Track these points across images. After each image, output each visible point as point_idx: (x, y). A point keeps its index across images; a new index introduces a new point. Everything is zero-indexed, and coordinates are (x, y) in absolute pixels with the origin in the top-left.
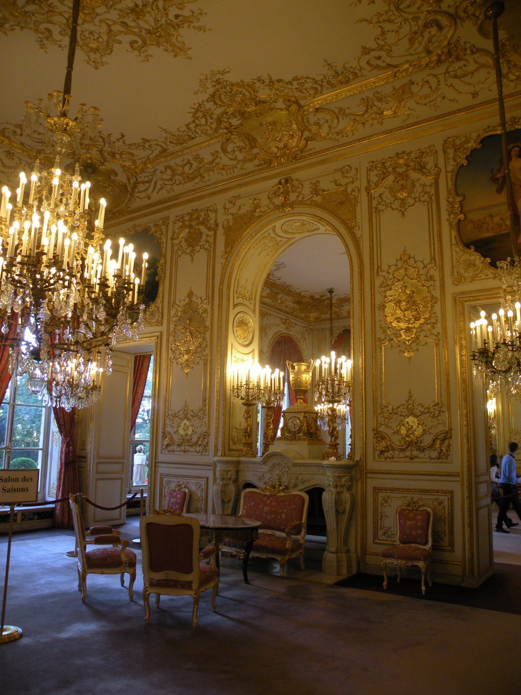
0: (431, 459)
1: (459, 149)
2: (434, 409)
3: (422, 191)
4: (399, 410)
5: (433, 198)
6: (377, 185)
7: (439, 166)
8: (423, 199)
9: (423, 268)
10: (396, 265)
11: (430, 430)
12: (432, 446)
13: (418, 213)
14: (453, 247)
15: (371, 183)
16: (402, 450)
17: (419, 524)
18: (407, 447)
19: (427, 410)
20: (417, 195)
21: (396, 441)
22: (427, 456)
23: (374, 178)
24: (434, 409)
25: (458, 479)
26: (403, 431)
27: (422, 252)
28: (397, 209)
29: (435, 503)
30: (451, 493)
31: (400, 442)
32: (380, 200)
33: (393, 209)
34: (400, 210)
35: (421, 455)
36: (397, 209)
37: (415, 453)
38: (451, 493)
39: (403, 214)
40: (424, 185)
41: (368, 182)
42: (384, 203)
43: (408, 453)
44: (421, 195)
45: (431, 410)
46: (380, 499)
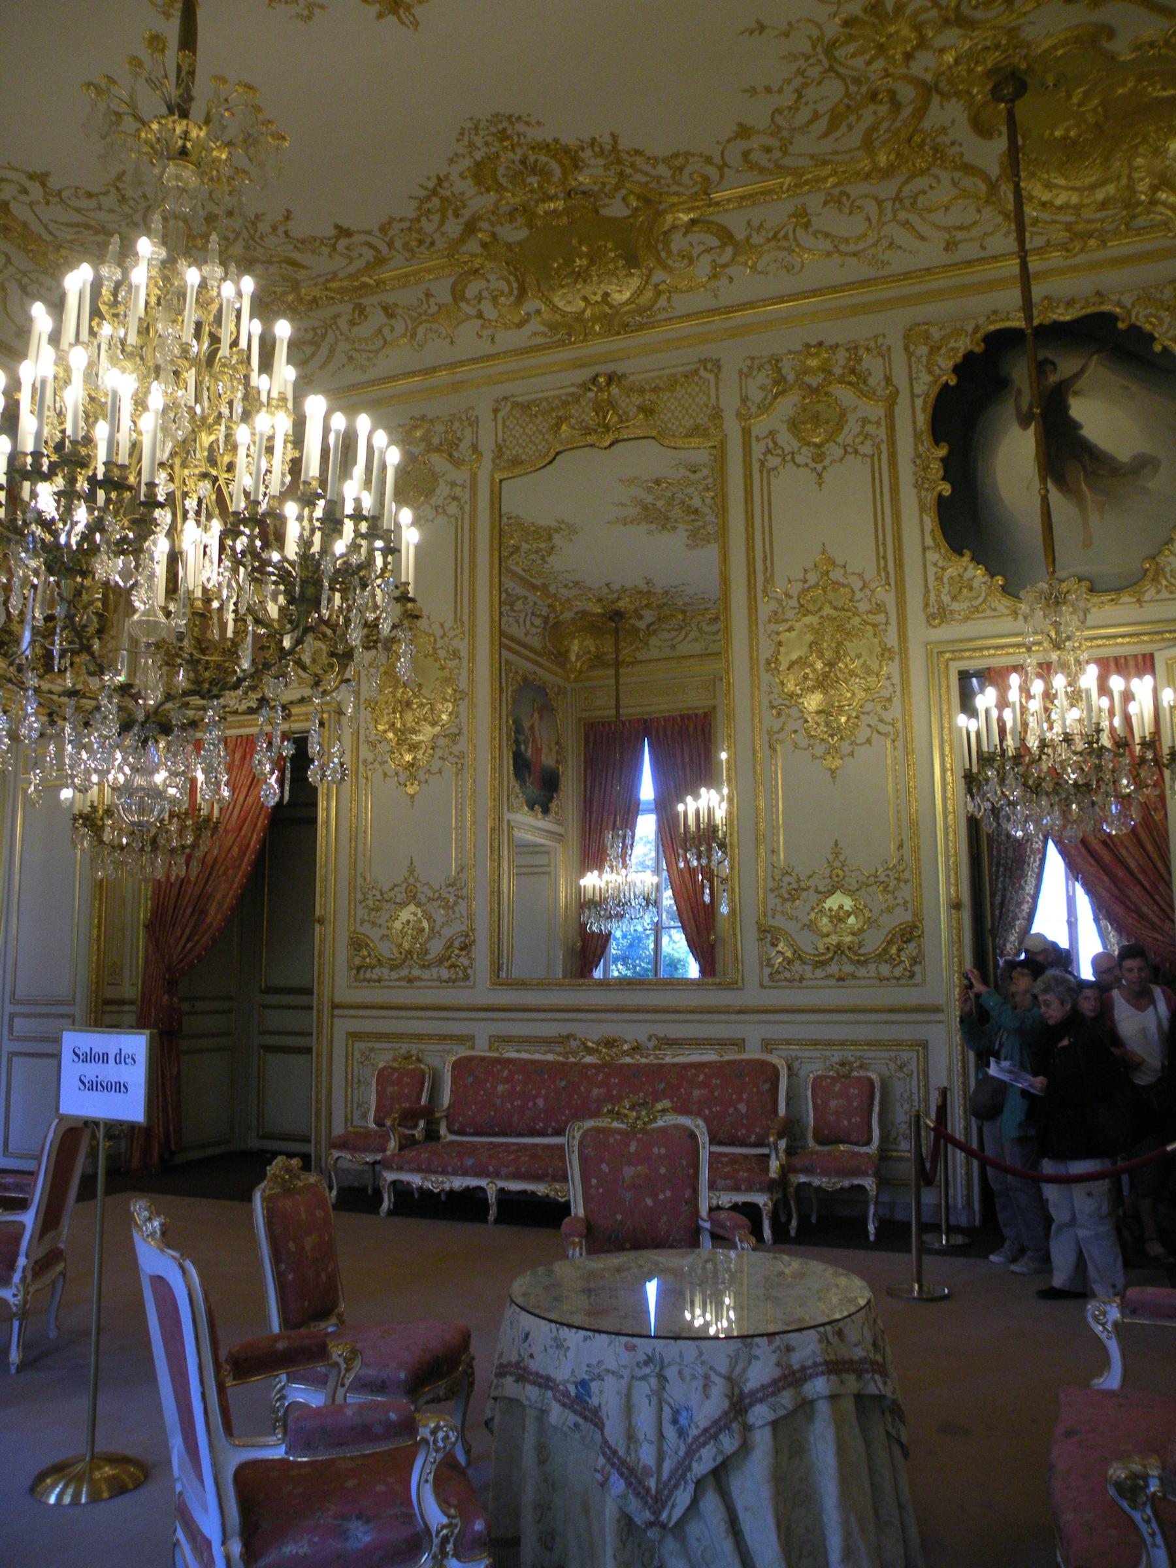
1: (939, 348)
3: (861, 433)
5: (884, 447)
7: (895, 381)
8: (860, 448)
10: (805, 581)
13: (851, 479)
14: (929, 554)
15: (749, 404)
18: (832, 959)
19: (872, 880)
20: (849, 441)
23: (756, 395)
25: (940, 1017)
27: (861, 558)
29: (892, 1066)
30: (924, 1045)
33: (799, 466)
36: (807, 465)
38: (924, 1045)
39: (820, 475)
40: (865, 421)
41: (744, 400)
44: (858, 440)
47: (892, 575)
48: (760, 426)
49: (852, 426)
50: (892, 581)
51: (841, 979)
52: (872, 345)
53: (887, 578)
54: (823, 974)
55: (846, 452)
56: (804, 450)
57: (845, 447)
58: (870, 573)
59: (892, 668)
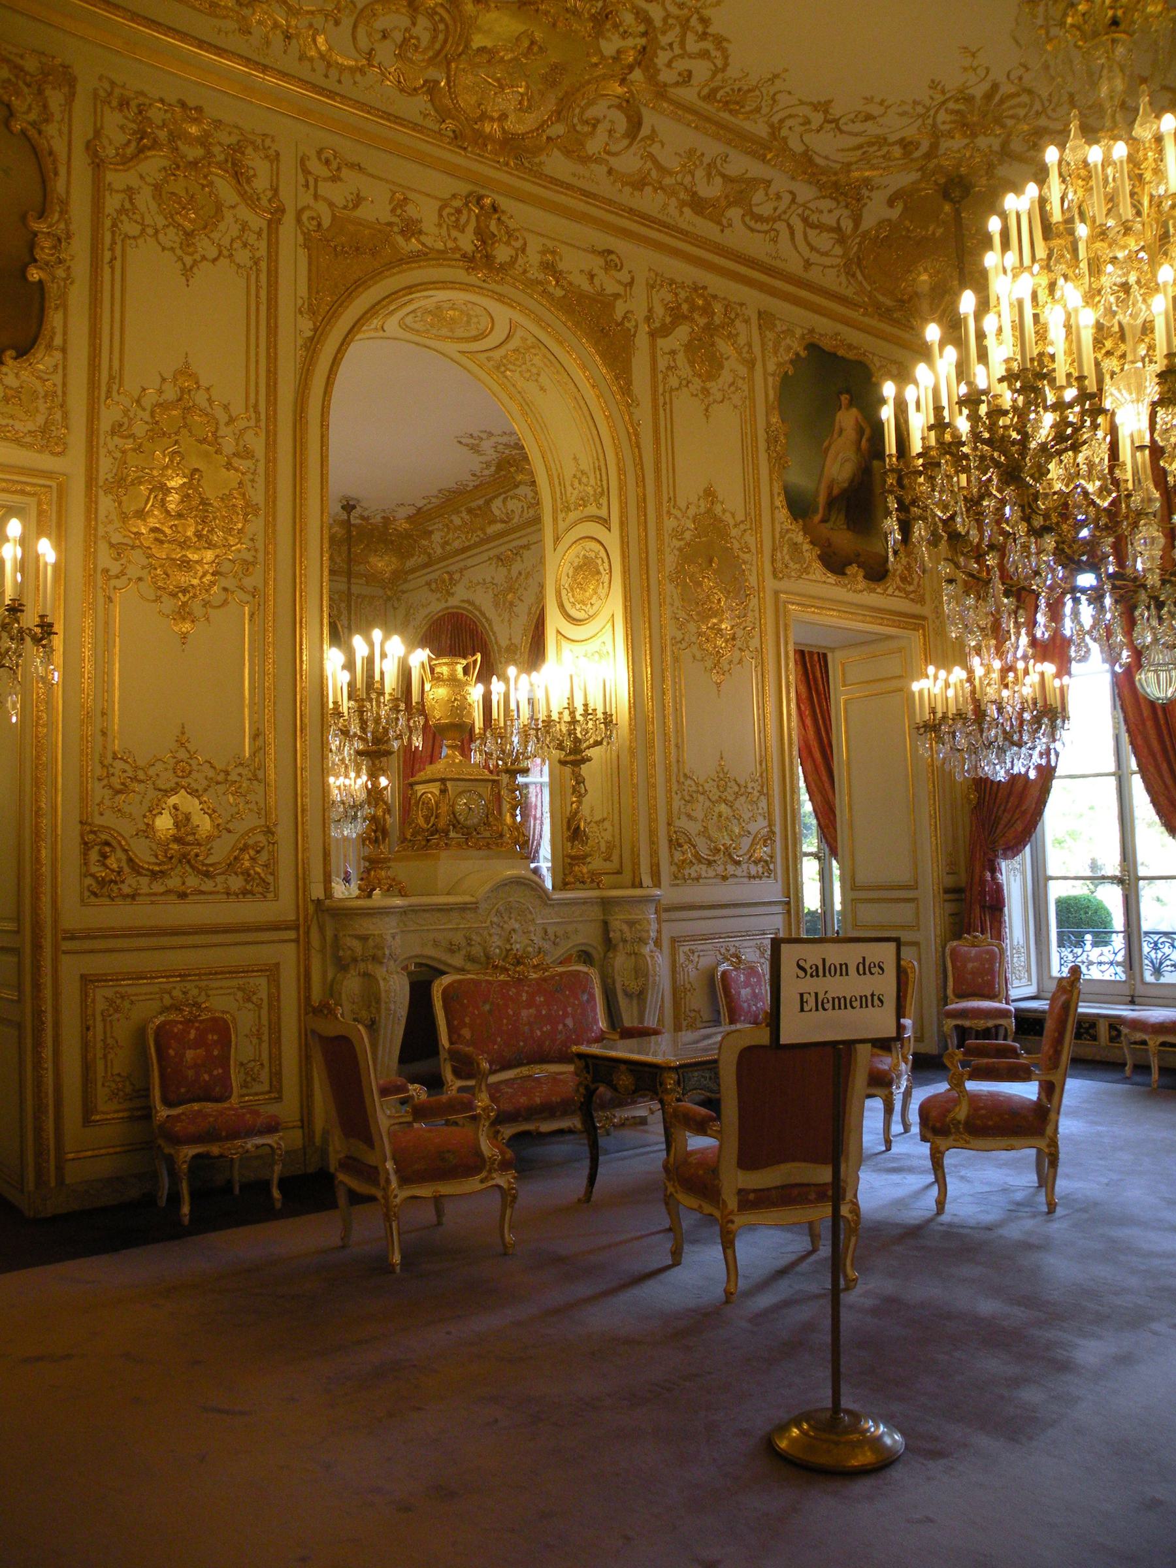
0: (228, 894)
2: (240, 775)
4: (152, 771)
6: (126, 161)
9: (227, 424)
11: (231, 826)
12: (232, 866)
16: (154, 875)
17: (216, 1053)
21: (143, 852)
22: (220, 888)
24: (240, 775)
26: (164, 823)
28: (172, 249)
31: (156, 856)
32: (127, 206)
34: (180, 259)
35: (208, 886)
36: (172, 249)
37: (193, 881)
42: (137, 217)
43: (173, 882)
45: (231, 778)
46: (101, 1005)
47: (263, 417)
48: (116, 178)
49: (228, 228)
50: (263, 424)
51: (183, 895)
52: (259, 141)
53: (258, 420)
54: (162, 889)
55: (220, 253)
56: (171, 231)
57: (219, 246)
58: (238, 408)
59: (256, 526)
